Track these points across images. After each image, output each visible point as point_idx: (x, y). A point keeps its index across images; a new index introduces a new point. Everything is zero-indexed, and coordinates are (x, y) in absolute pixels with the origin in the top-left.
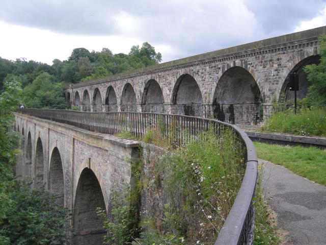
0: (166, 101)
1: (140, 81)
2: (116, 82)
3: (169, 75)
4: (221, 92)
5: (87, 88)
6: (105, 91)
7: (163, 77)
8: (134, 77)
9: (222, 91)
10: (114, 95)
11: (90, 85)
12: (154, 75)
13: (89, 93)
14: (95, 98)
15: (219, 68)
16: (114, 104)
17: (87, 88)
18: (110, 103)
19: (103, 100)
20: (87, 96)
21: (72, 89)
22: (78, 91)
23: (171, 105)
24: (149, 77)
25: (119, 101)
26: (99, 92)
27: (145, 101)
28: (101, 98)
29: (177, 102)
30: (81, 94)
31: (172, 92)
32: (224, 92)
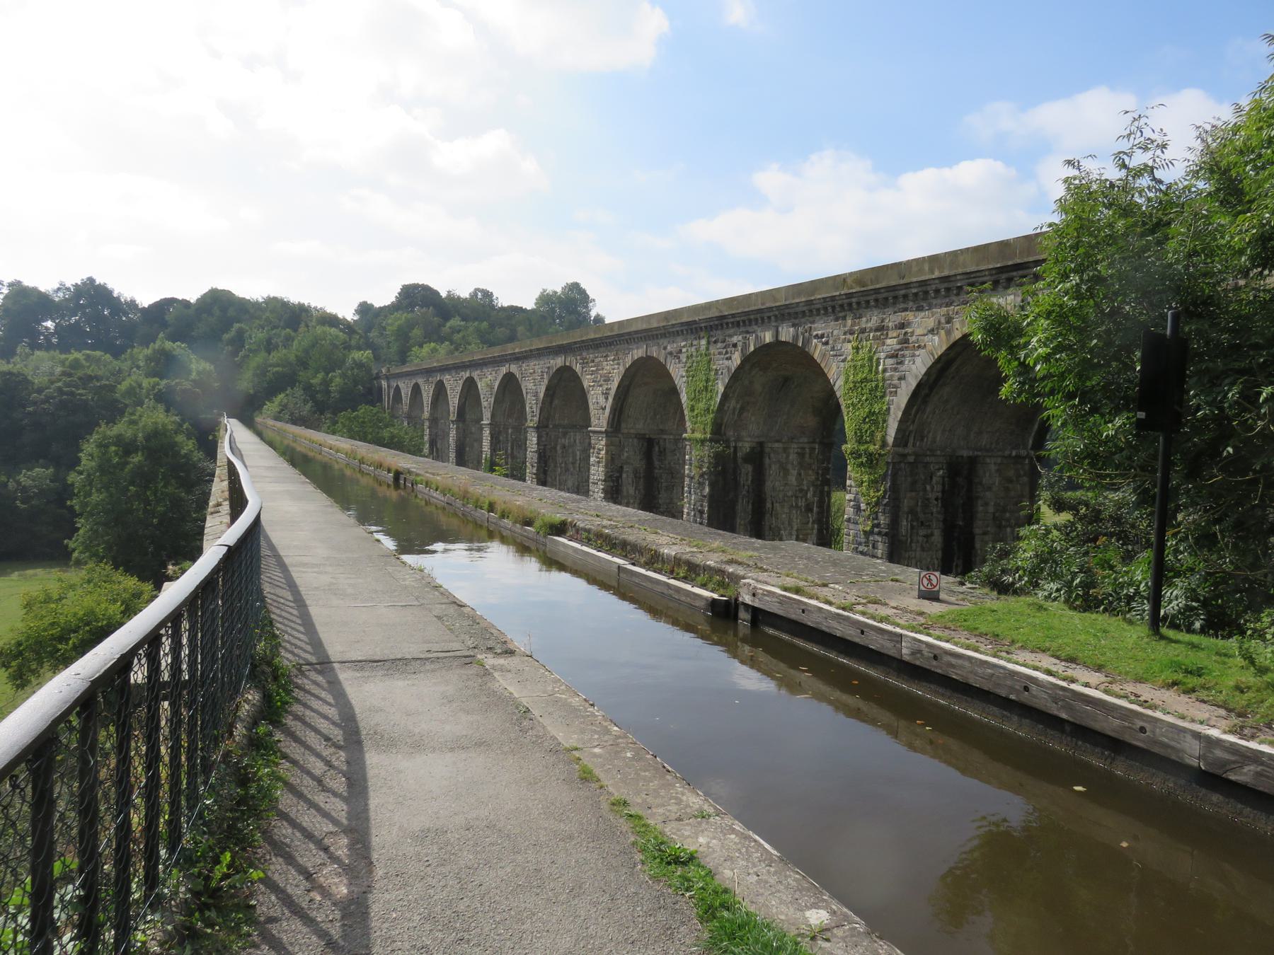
0: (594, 421)
4: (734, 409)
9: (738, 406)
15: (735, 345)
24: (559, 362)
29: (623, 425)
31: (610, 400)
32: (742, 409)
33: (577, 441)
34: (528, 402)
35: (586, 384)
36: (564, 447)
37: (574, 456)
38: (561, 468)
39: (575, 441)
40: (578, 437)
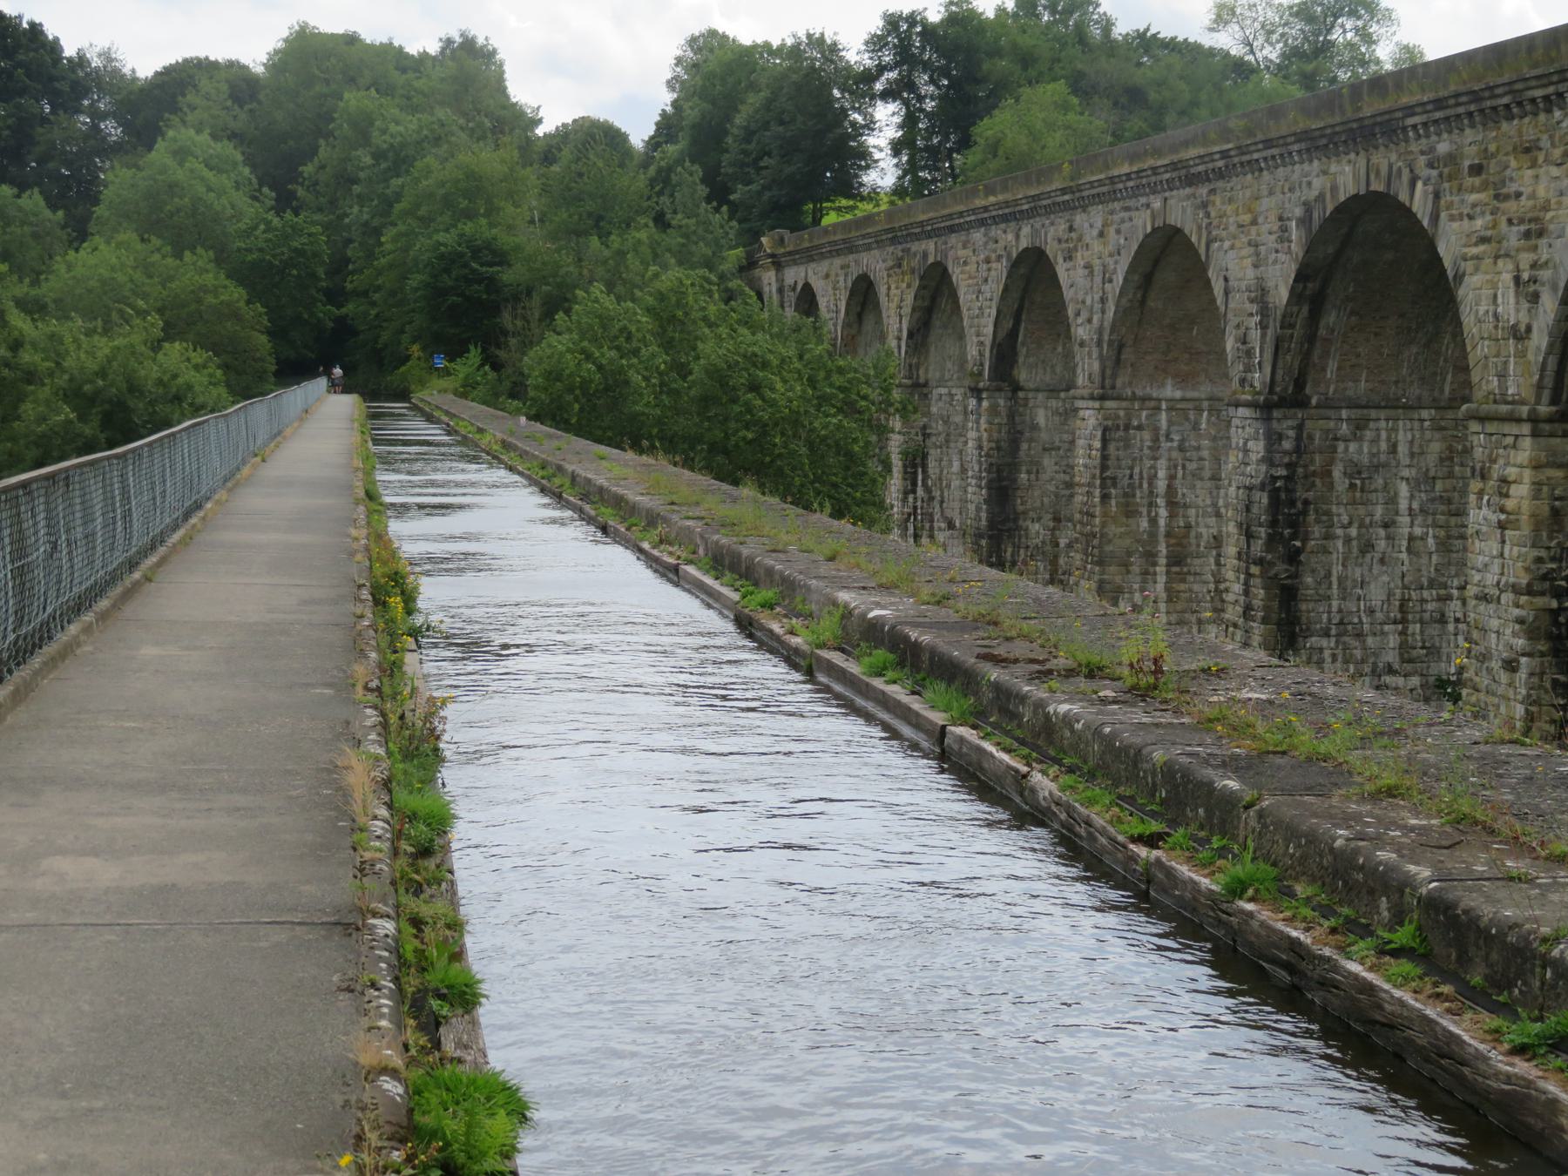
0: (1485, 382)
1: (1267, 203)
2: (1079, 219)
3: (1528, 150)
5: (875, 263)
6: (994, 289)
7: (1477, 170)
8: (1221, 175)
10: (1056, 321)
11: (894, 241)
12: (1384, 158)
13: (883, 299)
14: (919, 334)
16: (1053, 391)
17: (875, 263)
18: (1022, 375)
19: (972, 352)
20: (869, 324)
21: (778, 265)
22: (818, 285)
23: (1534, 419)
25: (1088, 367)
26: (954, 295)
27: (1300, 384)
28: (961, 337)
30: (833, 302)
33: (1402, 449)
34: (1233, 320)
35: (1447, 249)
36: (1354, 471)
37: (1392, 501)
38: (1348, 540)
39: (1393, 449)
40: (1403, 437)
